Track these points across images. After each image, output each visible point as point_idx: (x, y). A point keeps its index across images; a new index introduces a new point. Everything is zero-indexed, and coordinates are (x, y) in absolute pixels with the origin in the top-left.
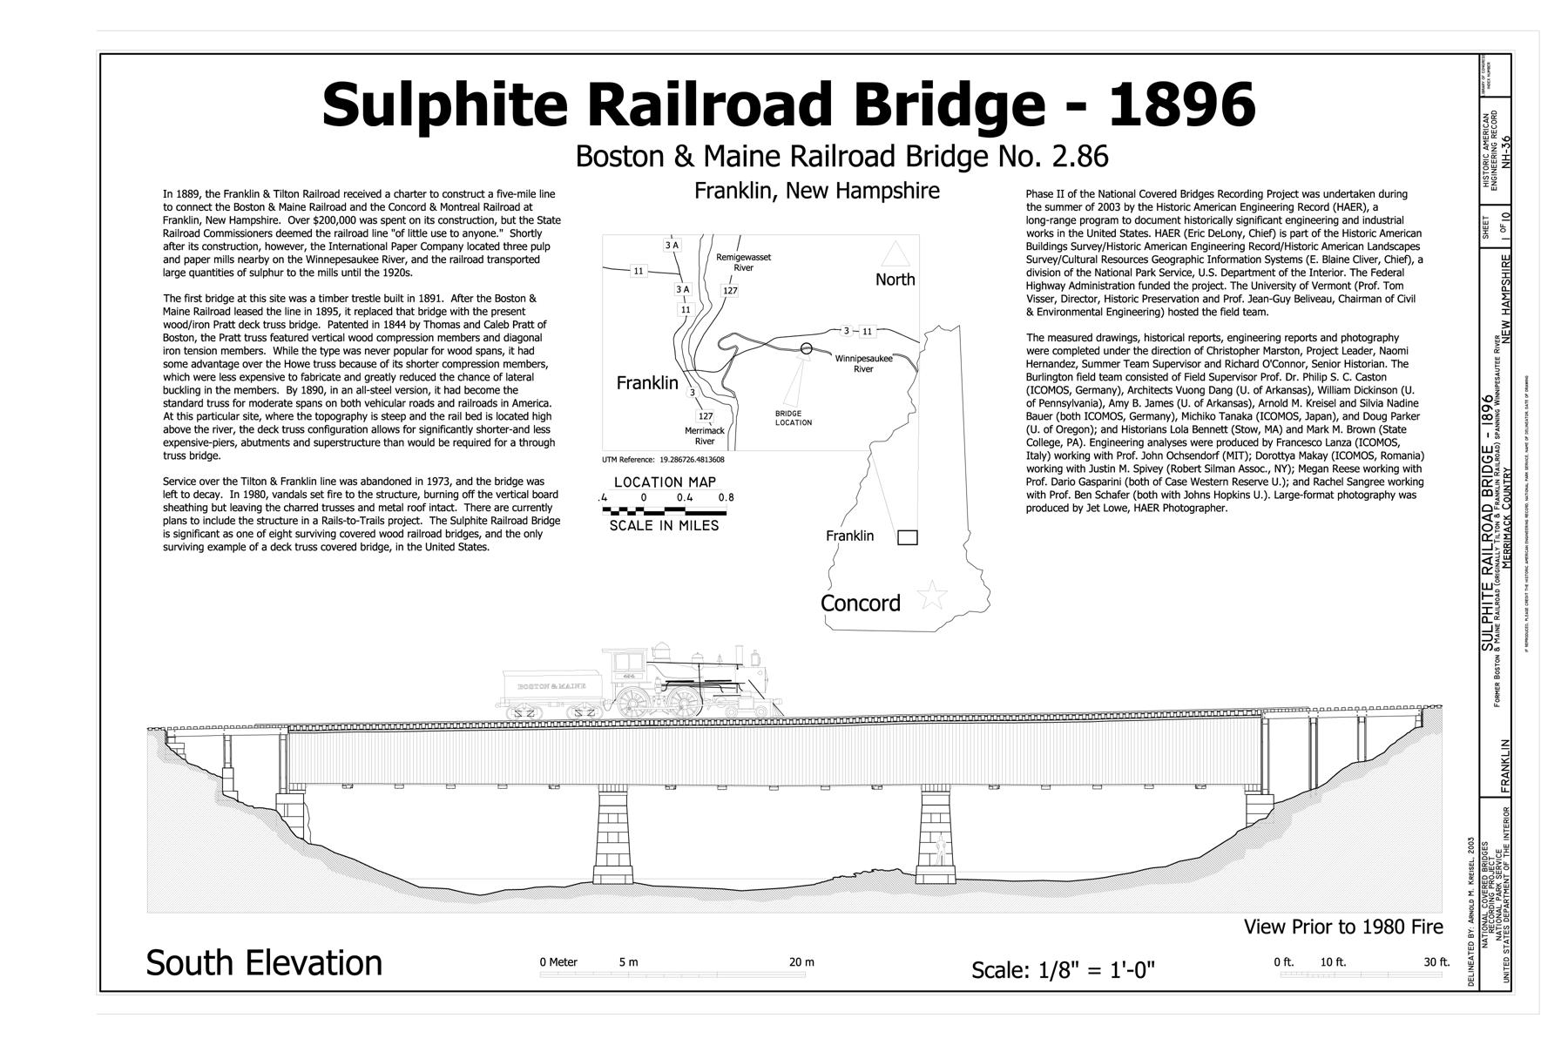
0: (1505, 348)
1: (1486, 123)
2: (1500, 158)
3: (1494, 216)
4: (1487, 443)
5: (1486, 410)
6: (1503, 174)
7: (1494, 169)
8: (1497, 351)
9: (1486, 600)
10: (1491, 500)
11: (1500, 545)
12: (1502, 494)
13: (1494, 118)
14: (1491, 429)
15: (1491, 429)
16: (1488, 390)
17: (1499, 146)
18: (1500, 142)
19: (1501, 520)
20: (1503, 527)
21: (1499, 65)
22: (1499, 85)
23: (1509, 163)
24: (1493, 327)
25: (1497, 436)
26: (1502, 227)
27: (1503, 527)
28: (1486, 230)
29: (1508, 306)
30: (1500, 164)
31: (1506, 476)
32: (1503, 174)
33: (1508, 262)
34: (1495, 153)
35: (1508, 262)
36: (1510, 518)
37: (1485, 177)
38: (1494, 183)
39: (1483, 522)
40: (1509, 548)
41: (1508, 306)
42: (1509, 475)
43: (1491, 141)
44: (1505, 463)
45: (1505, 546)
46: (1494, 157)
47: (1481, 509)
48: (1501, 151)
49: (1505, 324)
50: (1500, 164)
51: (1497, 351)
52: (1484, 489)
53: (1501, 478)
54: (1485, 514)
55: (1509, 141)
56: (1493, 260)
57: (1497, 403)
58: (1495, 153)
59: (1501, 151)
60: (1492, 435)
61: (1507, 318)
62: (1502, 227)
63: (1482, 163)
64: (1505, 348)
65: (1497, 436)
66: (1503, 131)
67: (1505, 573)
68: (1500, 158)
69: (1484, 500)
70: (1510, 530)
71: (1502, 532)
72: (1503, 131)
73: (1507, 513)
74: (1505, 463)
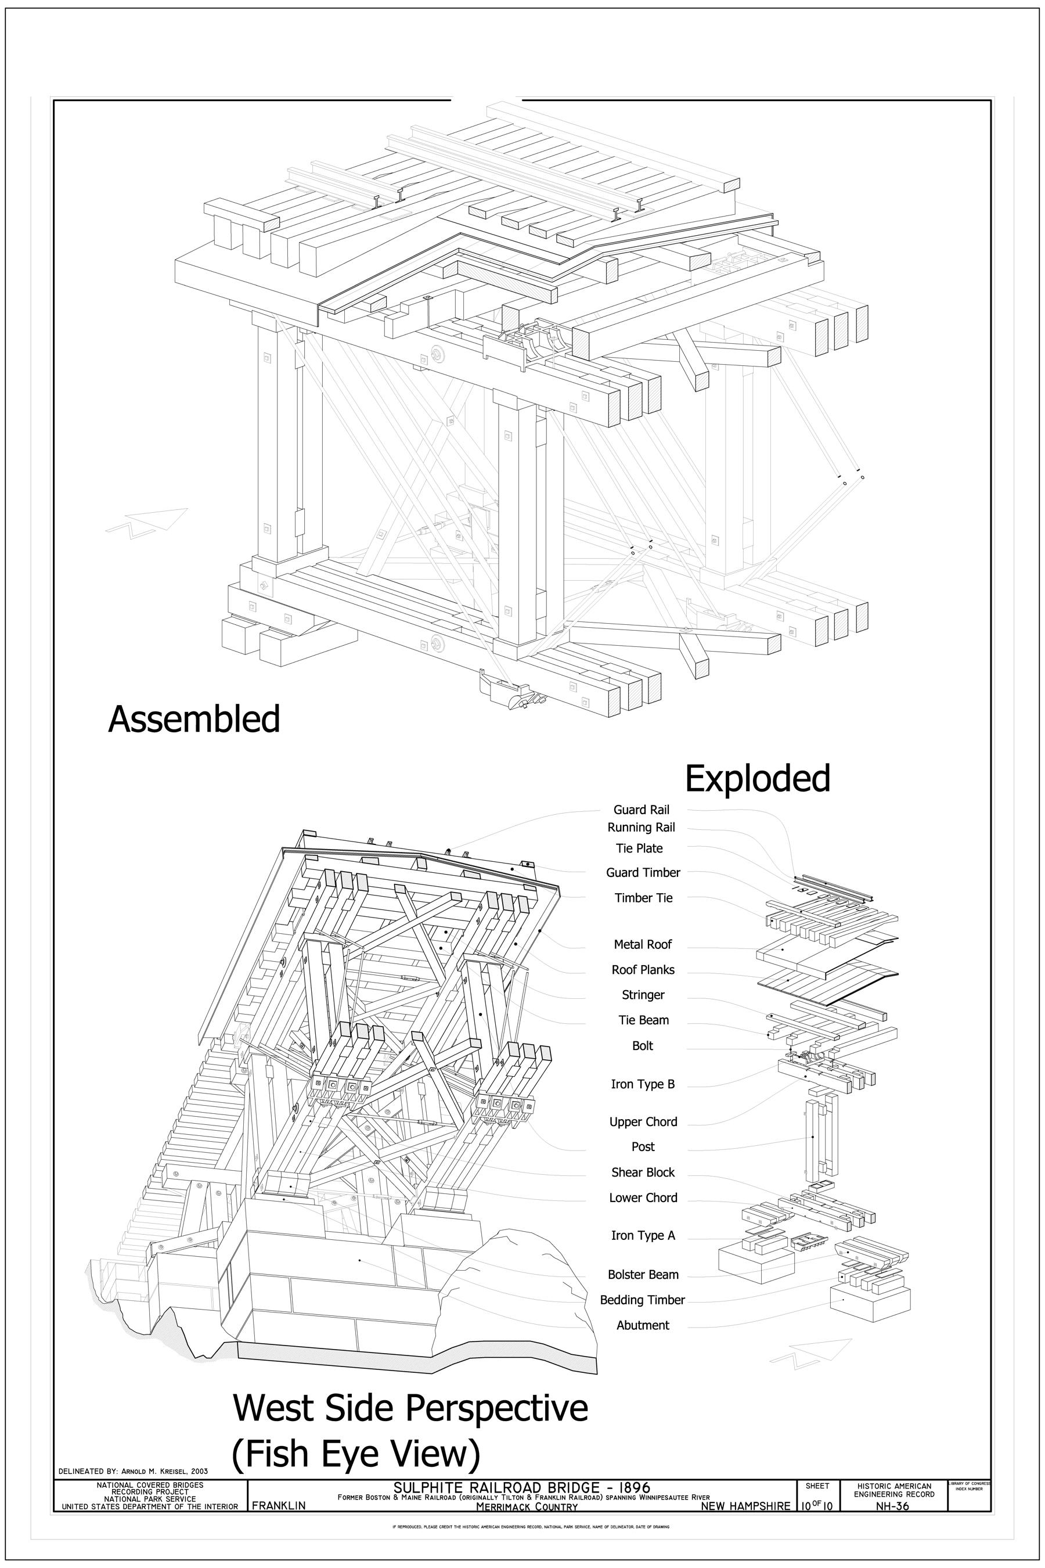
0: (697, 1505)
1: (921, 1486)
2: (887, 1500)
3: (829, 1494)
4: (602, 1487)
5: (635, 1486)
6: (871, 1503)
7: (876, 1495)
8: (694, 1497)
9: (445, 1486)
10: (544, 1491)
11: (500, 1500)
12: (551, 1502)
13: (927, 1494)
14: (616, 1491)
15: (616, 1491)
16: (655, 1488)
17: (899, 1499)
18: (904, 1500)
19: (525, 1501)
20: (518, 1503)
21: (979, 1499)
22: (960, 1499)
23: (882, 1509)
24: (719, 1493)
25: (609, 1498)
26: (818, 1503)
27: (518, 1503)
28: (816, 1486)
29: (740, 1509)
30: (880, 1500)
31: (569, 1506)
32: (871, 1503)
33: (783, 1508)
34: (892, 1495)
35: (783, 1508)
36: (526, 1510)
37: (868, 1485)
38: (862, 1495)
39: (523, 1483)
40: (497, 1509)
41: (740, 1509)
42: (570, 1510)
43: (904, 1491)
44: (583, 1505)
45: (499, 1506)
46: (888, 1494)
47: (536, 1481)
48: (893, 1501)
49: (721, 1505)
50: (880, 1500)
51: (694, 1497)
52: (556, 1484)
53: (567, 1501)
54: (531, 1485)
55: (904, 1509)
56: (784, 1493)
57: (642, 1497)
58: (892, 1495)
59: (893, 1501)
60: (610, 1493)
61: (727, 1508)
62: (818, 1503)
63: (882, 1482)
64: (697, 1505)
65: (609, 1498)
66: (914, 1503)
67: (471, 1505)
68: (887, 1500)
69: (545, 1485)
70: (515, 1510)
71: (513, 1503)
72: (914, 1503)
73: (532, 1508)
74: (583, 1505)
